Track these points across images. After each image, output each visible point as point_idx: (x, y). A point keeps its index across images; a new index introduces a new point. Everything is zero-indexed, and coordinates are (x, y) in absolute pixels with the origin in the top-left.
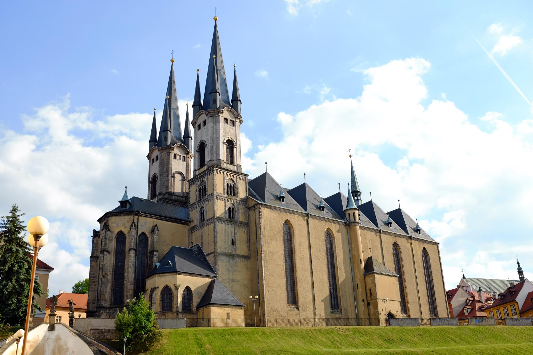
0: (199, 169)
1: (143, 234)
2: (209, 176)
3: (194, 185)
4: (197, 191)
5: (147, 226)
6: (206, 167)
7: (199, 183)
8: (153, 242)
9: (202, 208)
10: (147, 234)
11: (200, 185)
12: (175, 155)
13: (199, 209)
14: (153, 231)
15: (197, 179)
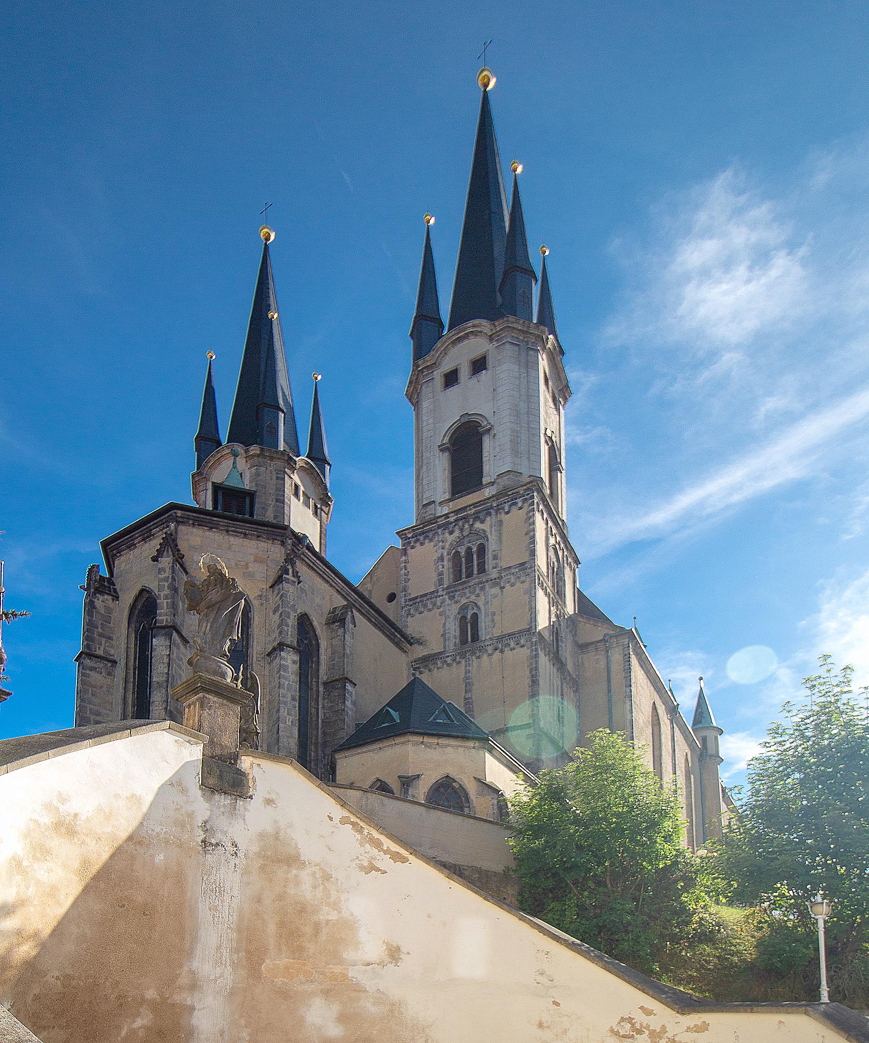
0: (450, 500)
1: (304, 622)
2: (503, 517)
3: (429, 545)
4: (441, 558)
5: (317, 600)
6: (487, 492)
7: (450, 538)
8: (340, 654)
9: (464, 608)
10: (315, 623)
11: (460, 542)
12: (297, 487)
13: (453, 610)
14: (337, 619)
15: (445, 526)
